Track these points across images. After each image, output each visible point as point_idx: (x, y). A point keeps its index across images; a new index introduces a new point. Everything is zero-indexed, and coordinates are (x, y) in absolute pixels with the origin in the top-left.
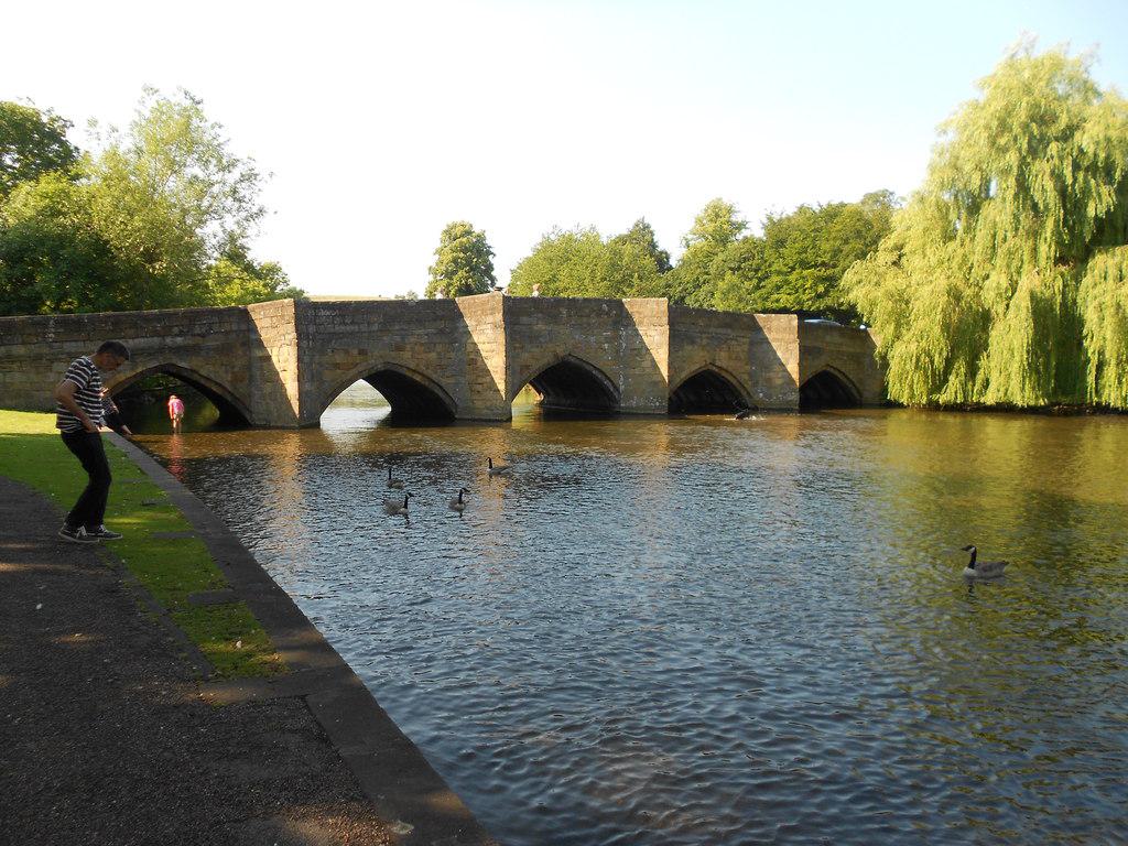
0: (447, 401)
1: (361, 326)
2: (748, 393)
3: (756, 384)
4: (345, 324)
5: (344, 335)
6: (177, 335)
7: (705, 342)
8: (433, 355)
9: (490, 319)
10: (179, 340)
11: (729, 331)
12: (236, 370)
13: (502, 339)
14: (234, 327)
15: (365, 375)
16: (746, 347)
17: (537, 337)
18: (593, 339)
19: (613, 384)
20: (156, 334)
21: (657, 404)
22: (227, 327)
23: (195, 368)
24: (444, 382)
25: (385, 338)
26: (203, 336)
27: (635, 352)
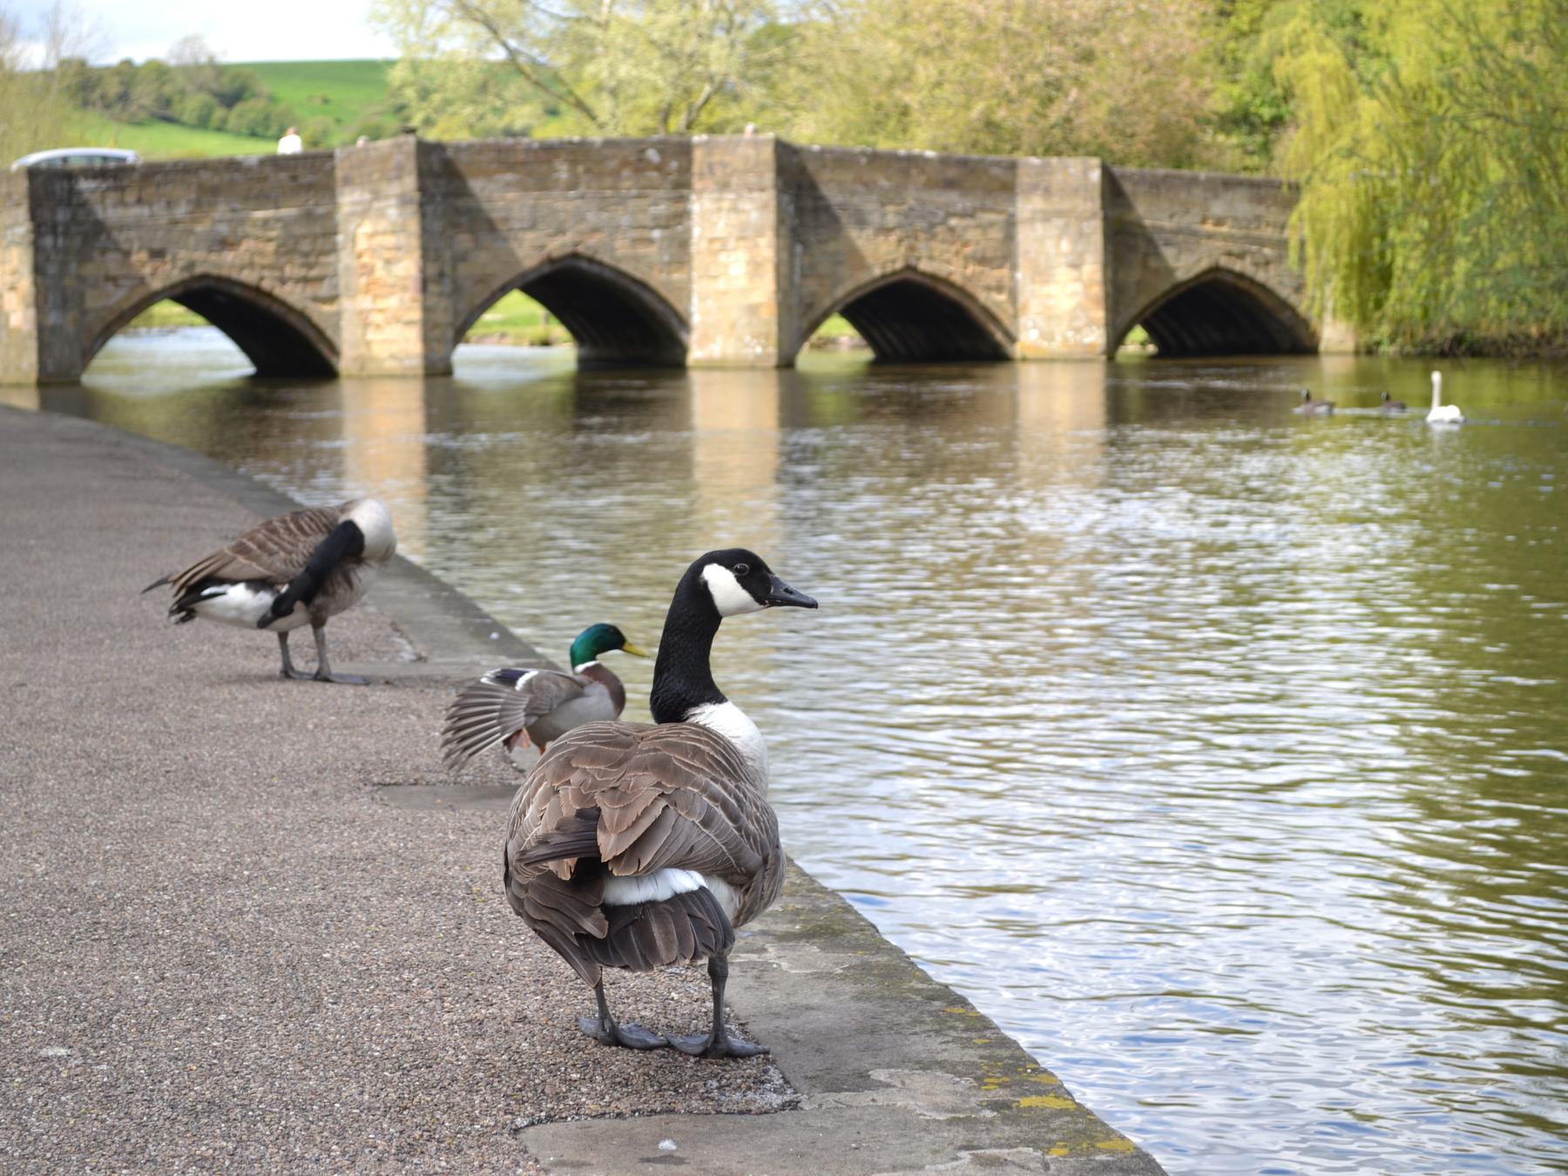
1: (156, 208)
9: (395, 189)
11: (953, 198)
13: (414, 225)
27: (717, 246)
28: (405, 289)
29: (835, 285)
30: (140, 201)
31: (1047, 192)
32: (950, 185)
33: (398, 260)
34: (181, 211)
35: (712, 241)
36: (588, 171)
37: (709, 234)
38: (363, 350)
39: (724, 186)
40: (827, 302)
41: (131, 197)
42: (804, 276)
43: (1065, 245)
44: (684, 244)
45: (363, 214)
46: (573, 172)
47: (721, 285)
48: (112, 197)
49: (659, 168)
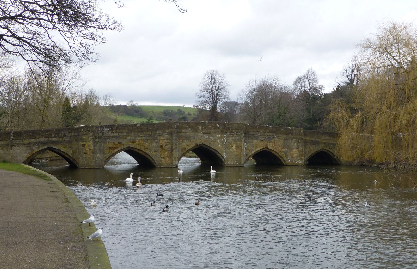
0: (153, 162)
1: (119, 134)
2: (284, 160)
3: (287, 156)
4: (113, 133)
5: (113, 137)
6: (53, 137)
7: (263, 139)
8: (147, 144)
10: (54, 139)
11: (274, 134)
12: (74, 149)
14: (73, 134)
15: (124, 150)
16: (282, 141)
17: (189, 137)
18: (212, 138)
19: (221, 155)
20: (46, 137)
21: (238, 163)
22: (70, 134)
23: (59, 149)
24: (151, 154)
25: (128, 138)
26: (62, 137)
27: (230, 143)
28: (169, 150)
29: (252, 151)
30: (116, 132)
31: (292, 134)
32: (274, 132)
33: (167, 145)
34: (124, 134)
35: (229, 142)
36: (205, 128)
37: (228, 141)
38: (160, 162)
39: (231, 132)
40: (250, 154)
41: (114, 132)
42: (246, 149)
43: (295, 144)
44: (223, 143)
45: (161, 136)
46: (202, 129)
47: (231, 151)
48: (111, 131)
49: (219, 128)
